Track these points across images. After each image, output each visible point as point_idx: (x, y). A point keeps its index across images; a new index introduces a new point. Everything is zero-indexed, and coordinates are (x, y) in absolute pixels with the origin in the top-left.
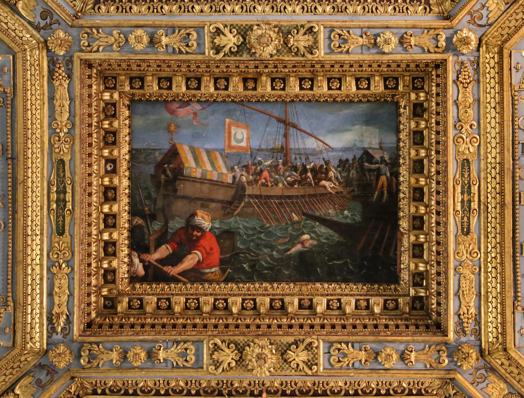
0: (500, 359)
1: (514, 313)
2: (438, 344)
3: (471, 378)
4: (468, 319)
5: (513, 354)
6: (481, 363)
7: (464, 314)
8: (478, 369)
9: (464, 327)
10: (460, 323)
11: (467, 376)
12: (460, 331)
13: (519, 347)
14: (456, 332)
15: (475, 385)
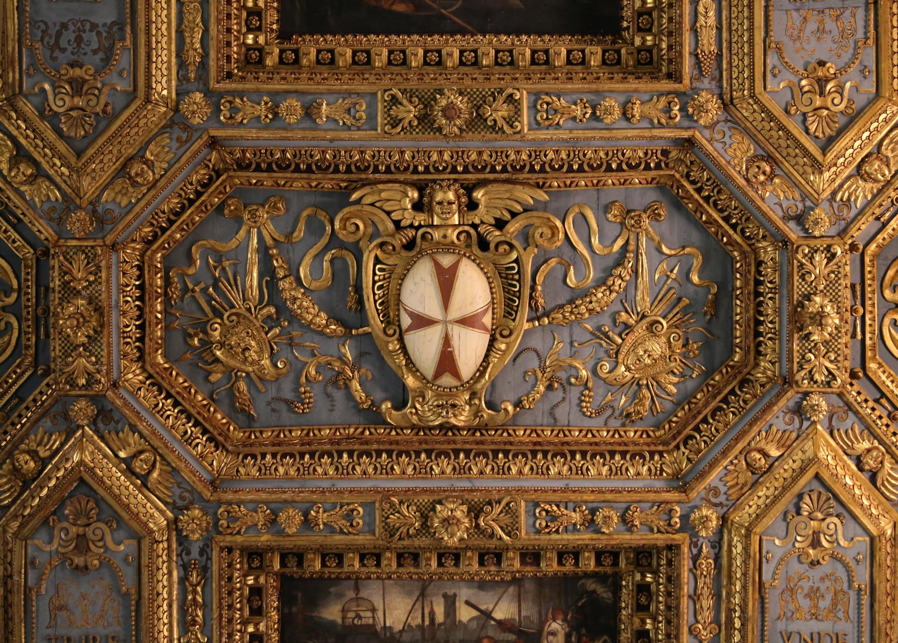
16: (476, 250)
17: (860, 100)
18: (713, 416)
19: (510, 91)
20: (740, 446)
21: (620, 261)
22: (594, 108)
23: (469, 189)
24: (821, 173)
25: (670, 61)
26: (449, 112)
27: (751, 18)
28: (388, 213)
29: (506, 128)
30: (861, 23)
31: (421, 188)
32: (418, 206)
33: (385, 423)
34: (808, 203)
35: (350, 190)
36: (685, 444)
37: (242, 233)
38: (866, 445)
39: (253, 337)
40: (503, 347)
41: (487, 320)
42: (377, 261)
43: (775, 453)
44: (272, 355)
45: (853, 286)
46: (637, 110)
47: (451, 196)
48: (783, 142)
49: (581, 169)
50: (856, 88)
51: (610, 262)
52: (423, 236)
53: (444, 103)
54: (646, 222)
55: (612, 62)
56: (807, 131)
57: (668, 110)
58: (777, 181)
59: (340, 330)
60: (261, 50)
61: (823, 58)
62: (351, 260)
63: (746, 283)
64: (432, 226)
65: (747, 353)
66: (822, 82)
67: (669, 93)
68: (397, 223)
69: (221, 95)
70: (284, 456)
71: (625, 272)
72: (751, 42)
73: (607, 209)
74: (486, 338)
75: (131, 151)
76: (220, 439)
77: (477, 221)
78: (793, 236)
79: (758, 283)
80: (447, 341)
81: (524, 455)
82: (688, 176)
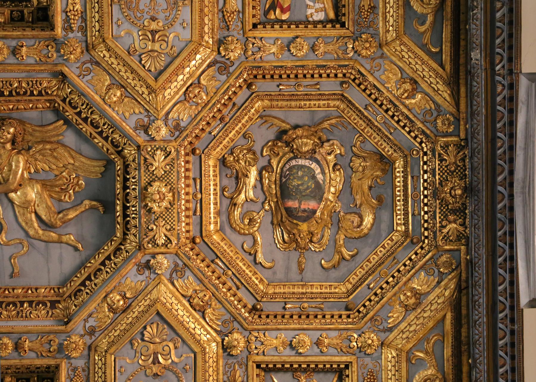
0: (102, 52)
1: (111, 5)
2: (46, 39)
3: (78, 72)
4: (74, 15)
5: (110, 43)
6: (87, 57)
7: (70, 11)
8: (84, 63)
9: (71, 24)
10: (67, 20)
11: (74, 69)
12: (68, 28)
13: (117, 38)
14: (64, 29)
15: (81, 77)
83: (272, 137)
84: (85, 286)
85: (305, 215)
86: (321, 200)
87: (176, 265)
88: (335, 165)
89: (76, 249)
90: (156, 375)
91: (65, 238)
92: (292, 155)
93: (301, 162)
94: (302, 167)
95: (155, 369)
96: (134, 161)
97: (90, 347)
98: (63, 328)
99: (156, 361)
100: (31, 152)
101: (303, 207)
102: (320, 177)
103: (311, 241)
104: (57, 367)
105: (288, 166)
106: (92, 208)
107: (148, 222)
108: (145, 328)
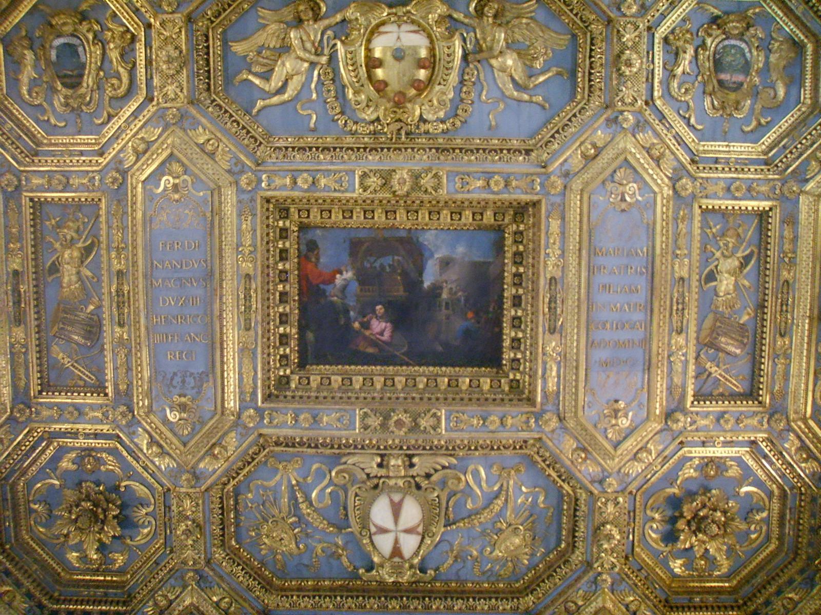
16: (414, 489)
17: (638, 421)
18: (548, 579)
19: (434, 411)
20: (562, 600)
21: (497, 496)
22: (485, 420)
23: (410, 457)
24: (613, 460)
25: (530, 392)
26: (399, 423)
27: (577, 375)
28: (363, 469)
29: (432, 432)
30: (640, 380)
31: (382, 456)
32: (380, 465)
33: (361, 579)
34: (606, 474)
35: (340, 456)
36: (532, 593)
37: (278, 477)
38: (631, 598)
39: (286, 533)
40: (429, 542)
41: (420, 529)
42: (356, 495)
43: (580, 603)
44: (296, 543)
45: (629, 512)
46: (510, 421)
47: (400, 462)
48: (592, 442)
49: (476, 449)
50: (635, 415)
51: (492, 496)
52: (384, 482)
53: (396, 418)
54: (513, 472)
55: (496, 387)
56: (607, 437)
57: (527, 422)
58: (588, 462)
59: (336, 530)
60: (288, 377)
61: (617, 398)
62: (341, 493)
63: (569, 508)
64: (388, 477)
65: (568, 544)
66: (616, 411)
67: (527, 413)
68: (368, 475)
69: (264, 410)
70: (304, 597)
71: (499, 502)
72: (576, 387)
73: (491, 467)
74: (419, 538)
75: (214, 441)
76: (268, 587)
77: (415, 474)
78: (596, 492)
79: (575, 510)
80: (396, 541)
81: (440, 599)
82: (538, 453)
83: (706, 21)
84: (554, 138)
85: (735, 86)
86: (747, 75)
87: (639, 122)
88: (758, 47)
89: (543, 107)
90: (623, 211)
91: (534, 99)
92: (724, 36)
93: (733, 42)
94: (734, 46)
95: (623, 206)
96: (601, 34)
97: (565, 187)
98: (543, 170)
99: (623, 200)
100: (510, 26)
101: (734, 79)
102: (748, 55)
103: (736, 109)
104: (539, 202)
105: (721, 45)
106: (559, 74)
107: (619, 84)
108: (615, 171)
